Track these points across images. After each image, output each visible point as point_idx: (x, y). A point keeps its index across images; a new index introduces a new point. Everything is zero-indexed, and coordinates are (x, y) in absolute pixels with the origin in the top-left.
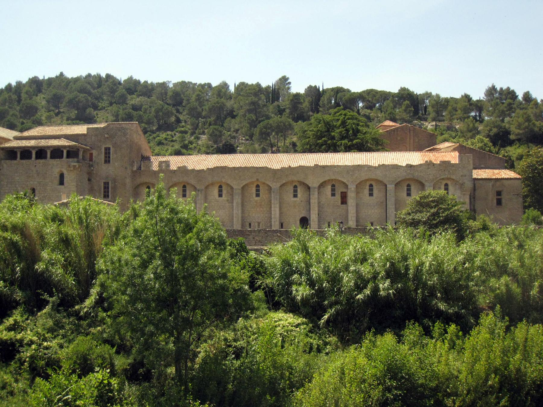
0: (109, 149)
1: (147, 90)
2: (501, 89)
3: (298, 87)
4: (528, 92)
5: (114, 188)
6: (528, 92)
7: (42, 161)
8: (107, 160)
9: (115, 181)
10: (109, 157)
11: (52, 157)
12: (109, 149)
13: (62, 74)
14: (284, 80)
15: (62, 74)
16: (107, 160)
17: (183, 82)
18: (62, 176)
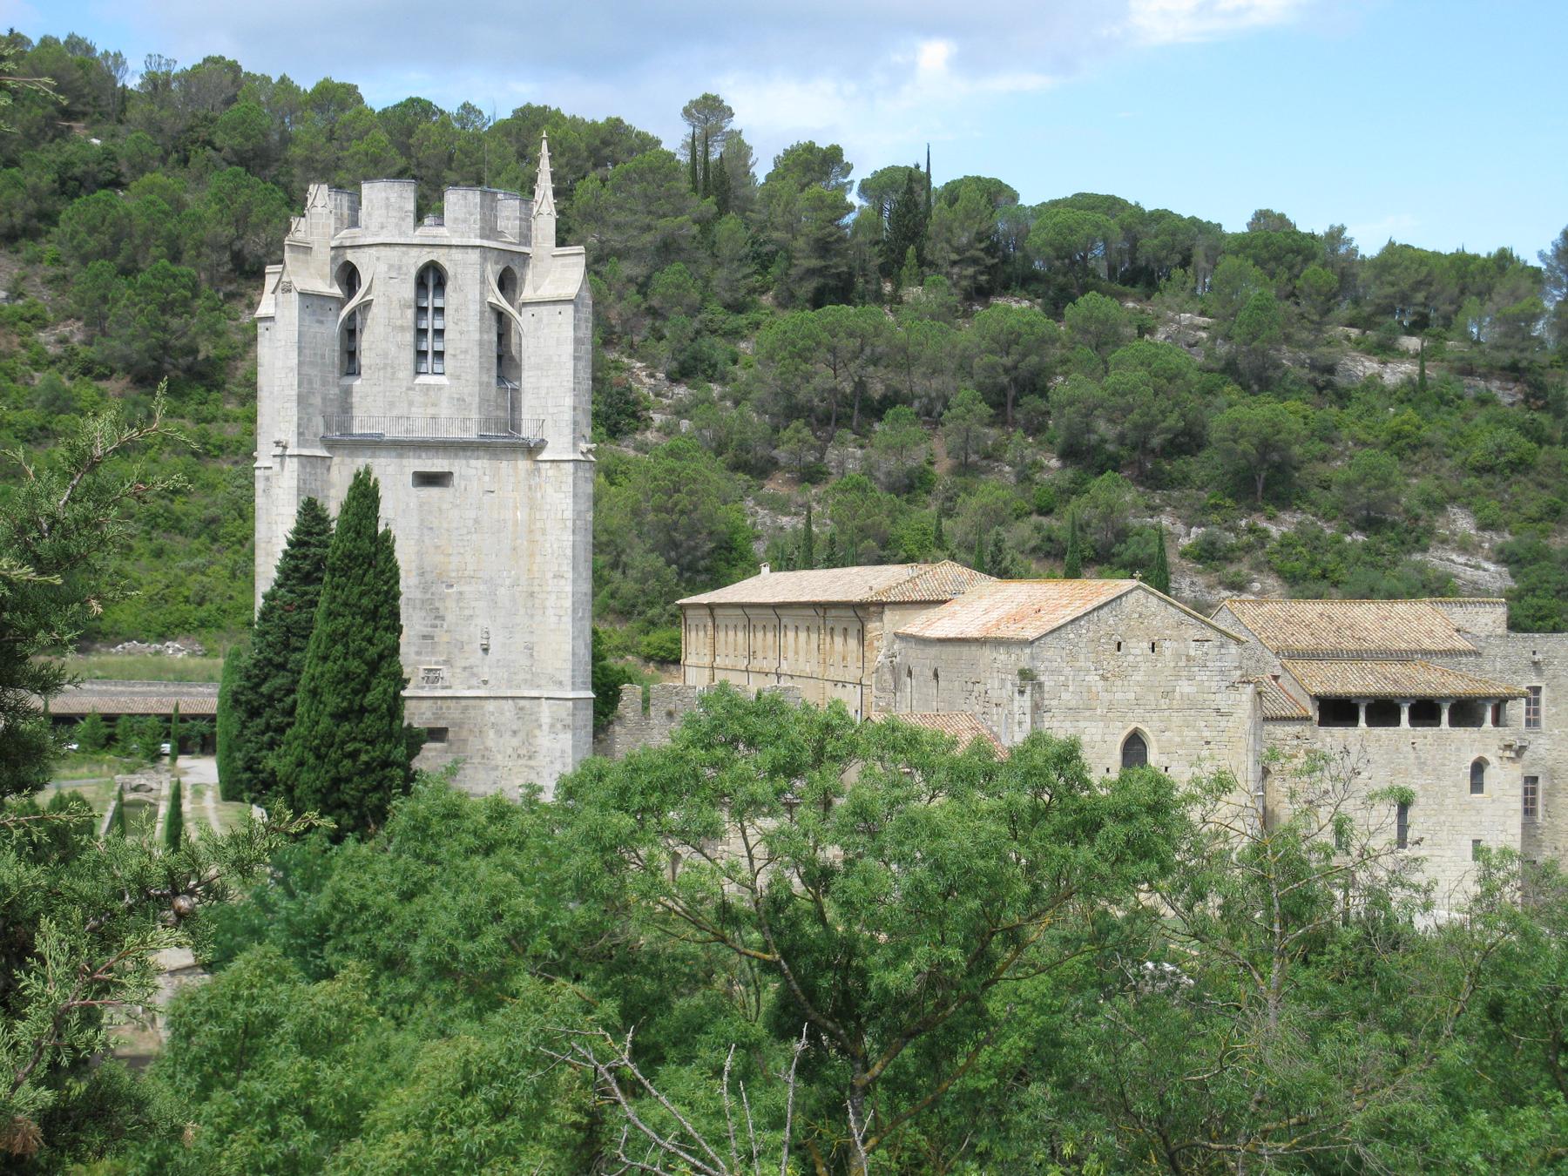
5: (1550, 794)
10: (1536, 712)
18: (1478, 768)
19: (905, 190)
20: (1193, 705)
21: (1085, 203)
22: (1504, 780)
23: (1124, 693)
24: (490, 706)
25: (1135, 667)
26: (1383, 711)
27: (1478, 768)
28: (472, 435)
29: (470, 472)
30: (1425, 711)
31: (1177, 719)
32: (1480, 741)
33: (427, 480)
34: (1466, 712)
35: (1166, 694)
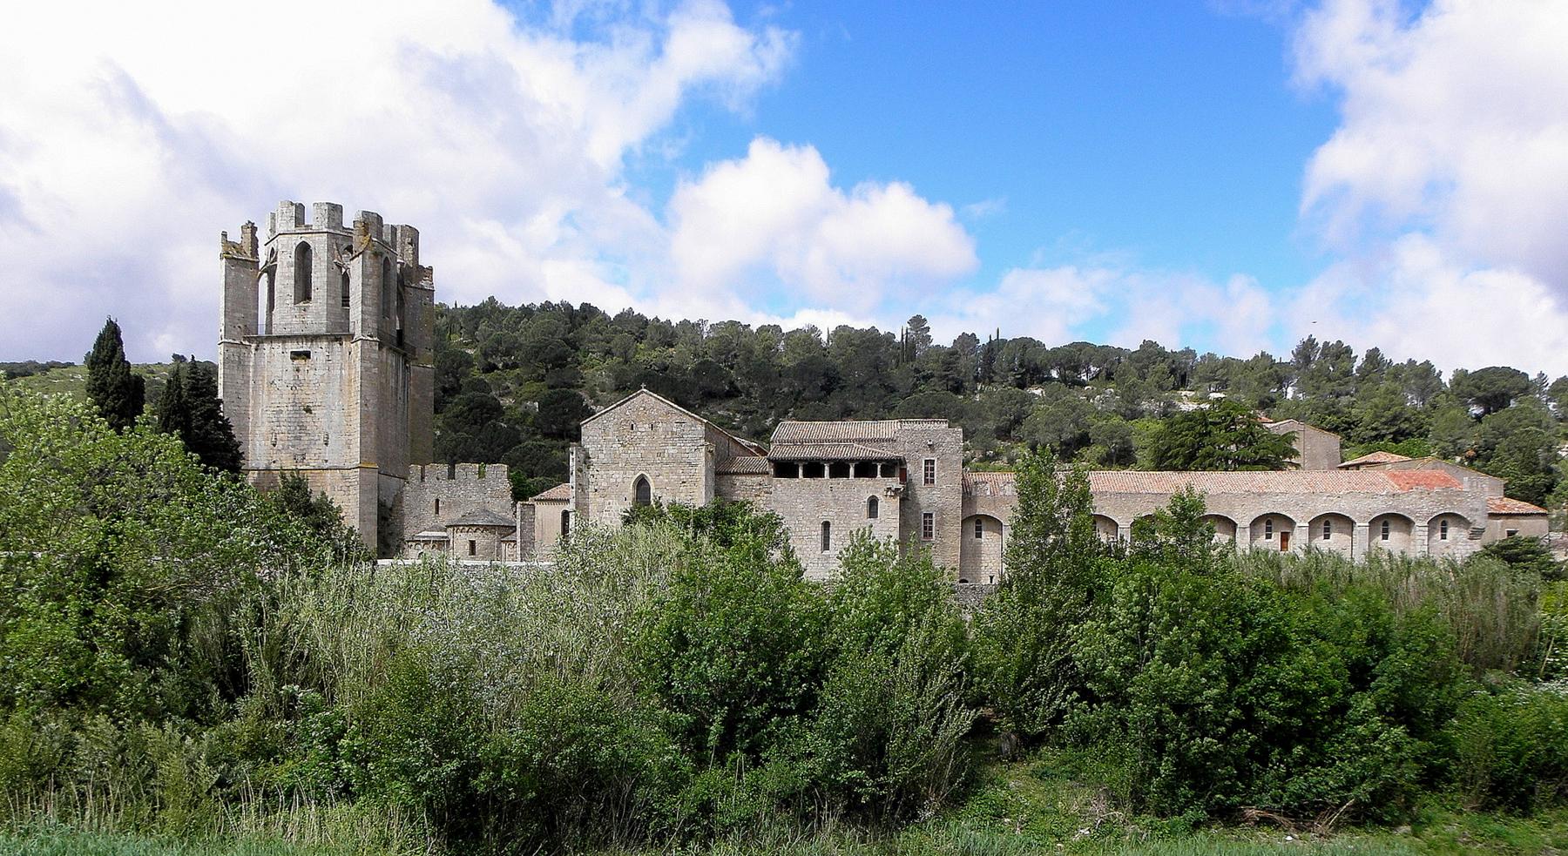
0: (932, 462)
1: (666, 334)
2: (1326, 344)
3: (943, 335)
4: (1377, 350)
5: (941, 523)
6: (1377, 350)
7: (842, 480)
8: (929, 480)
9: (941, 511)
11: (857, 475)
12: (932, 462)
13: (492, 299)
14: (918, 322)
15: (492, 299)
16: (929, 480)
17: (733, 323)
18: (873, 502)
19: (995, 346)
20: (676, 461)
21: (1074, 345)
22: (889, 509)
23: (633, 454)
24: (328, 474)
25: (642, 439)
26: (814, 469)
27: (873, 502)
28: (323, 331)
29: (319, 351)
30: (839, 469)
31: (665, 469)
32: (879, 486)
33: (296, 355)
34: (866, 469)
35: (659, 455)
